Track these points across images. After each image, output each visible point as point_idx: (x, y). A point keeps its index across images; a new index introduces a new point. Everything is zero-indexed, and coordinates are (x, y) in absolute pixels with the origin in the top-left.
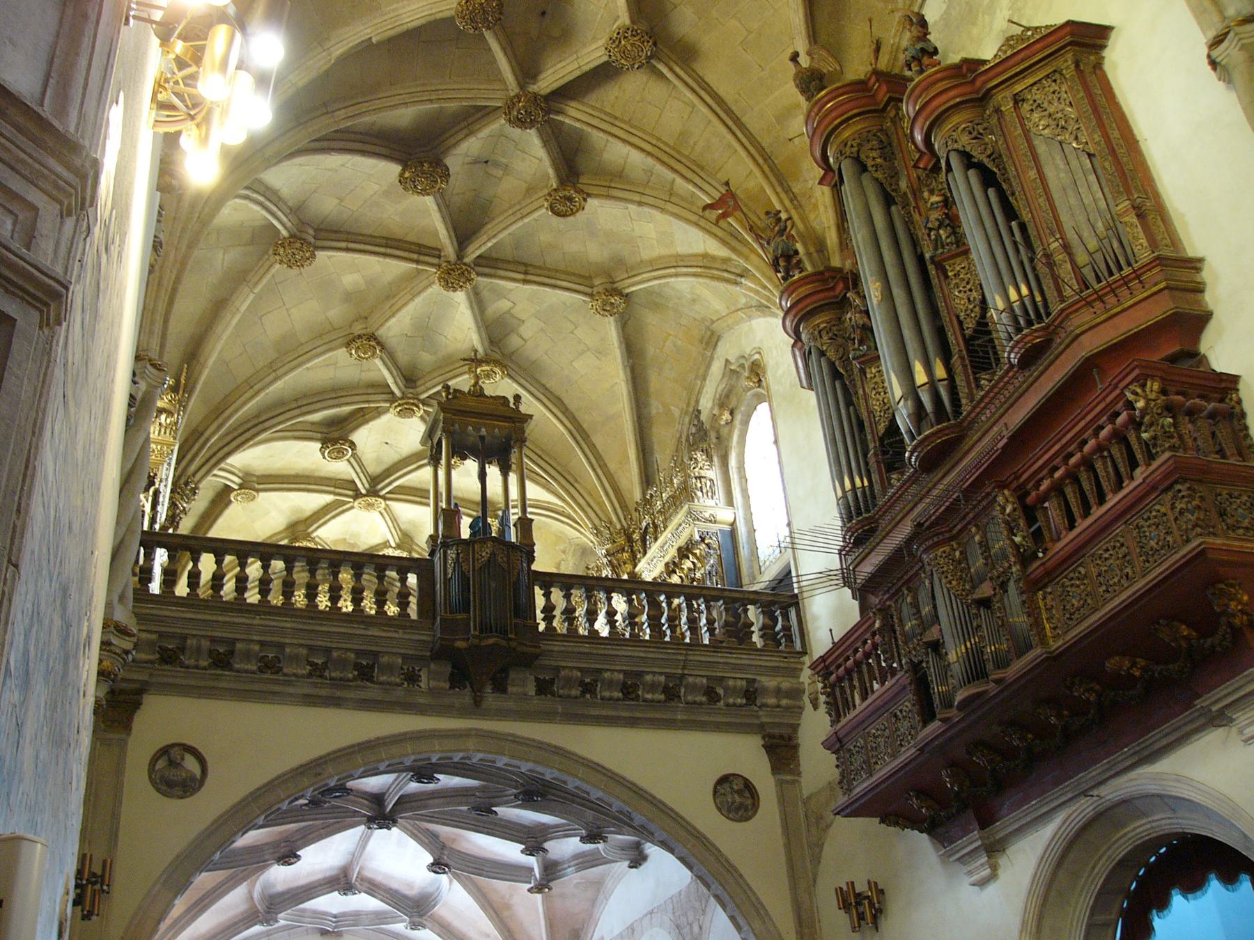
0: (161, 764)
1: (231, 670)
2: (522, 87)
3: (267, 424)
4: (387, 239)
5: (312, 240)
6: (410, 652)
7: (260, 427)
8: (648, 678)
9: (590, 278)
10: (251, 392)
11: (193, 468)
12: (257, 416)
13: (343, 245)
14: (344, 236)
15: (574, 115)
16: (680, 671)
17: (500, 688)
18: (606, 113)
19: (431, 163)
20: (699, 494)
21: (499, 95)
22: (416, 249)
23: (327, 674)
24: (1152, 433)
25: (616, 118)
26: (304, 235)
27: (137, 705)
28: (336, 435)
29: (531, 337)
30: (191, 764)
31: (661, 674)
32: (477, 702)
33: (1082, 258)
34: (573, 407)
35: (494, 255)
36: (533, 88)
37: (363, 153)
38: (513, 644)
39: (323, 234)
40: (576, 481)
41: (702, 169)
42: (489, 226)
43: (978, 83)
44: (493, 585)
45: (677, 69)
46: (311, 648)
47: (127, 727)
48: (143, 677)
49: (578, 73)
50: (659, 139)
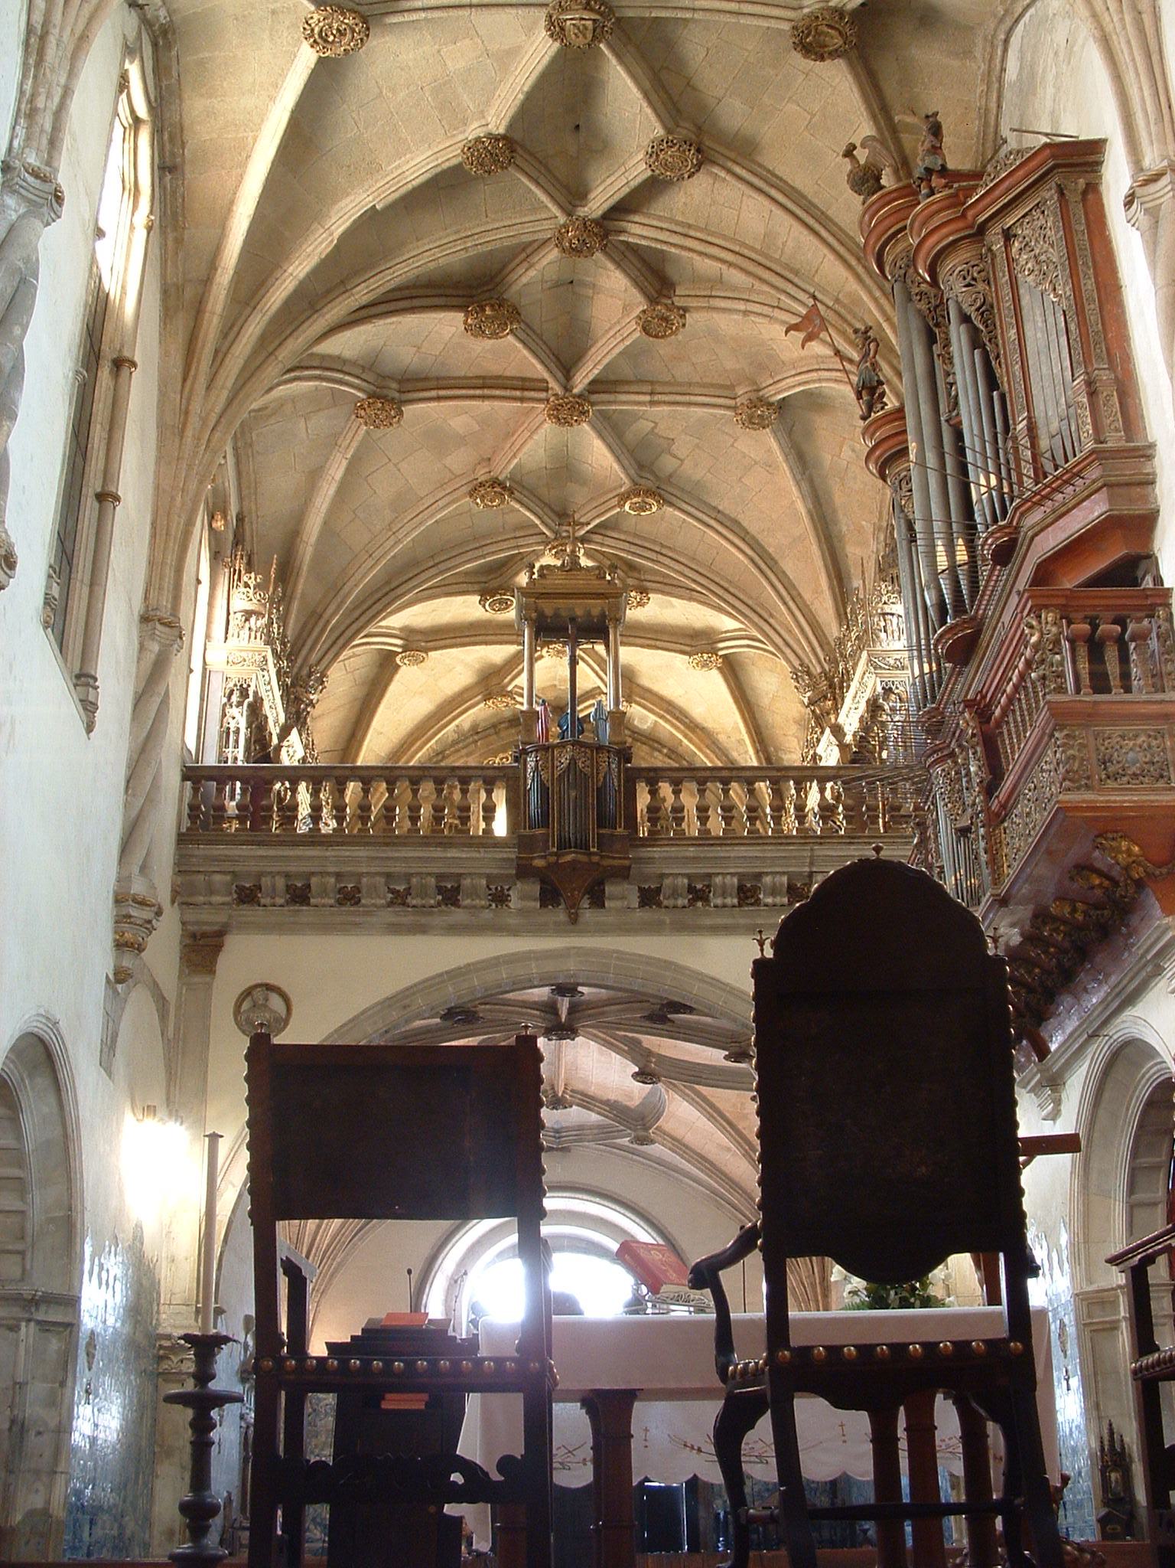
0: (245, 1006)
1: (308, 904)
2: (569, 214)
3: (399, 591)
4: (484, 378)
5: (397, 395)
6: (496, 871)
7: (392, 595)
8: (768, 880)
9: (732, 387)
10: (370, 562)
11: (314, 658)
12: (388, 583)
13: (433, 393)
14: (433, 384)
15: (637, 231)
16: (807, 869)
17: (598, 901)
18: (678, 223)
19: (492, 306)
20: (883, 635)
21: (546, 225)
22: (522, 387)
23: (409, 900)
24: (1041, 673)
25: (690, 226)
26: (385, 392)
27: (218, 948)
28: (494, 584)
29: (687, 459)
30: (276, 1003)
31: (784, 873)
32: (574, 919)
33: (1044, 443)
34: (753, 529)
35: (612, 377)
36: (582, 212)
37: (412, 310)
38: (595, 859)
39: (410, 386)
40: (771, 616)
41: (796, 273)
42: (593, 350)
43: (970, 214)
44: (573, 794)
45: (738, 170)
46: (389, 876)
47: (212, 971)
48: (221, 918)
49: (627, 190)
50: (743, 244)
